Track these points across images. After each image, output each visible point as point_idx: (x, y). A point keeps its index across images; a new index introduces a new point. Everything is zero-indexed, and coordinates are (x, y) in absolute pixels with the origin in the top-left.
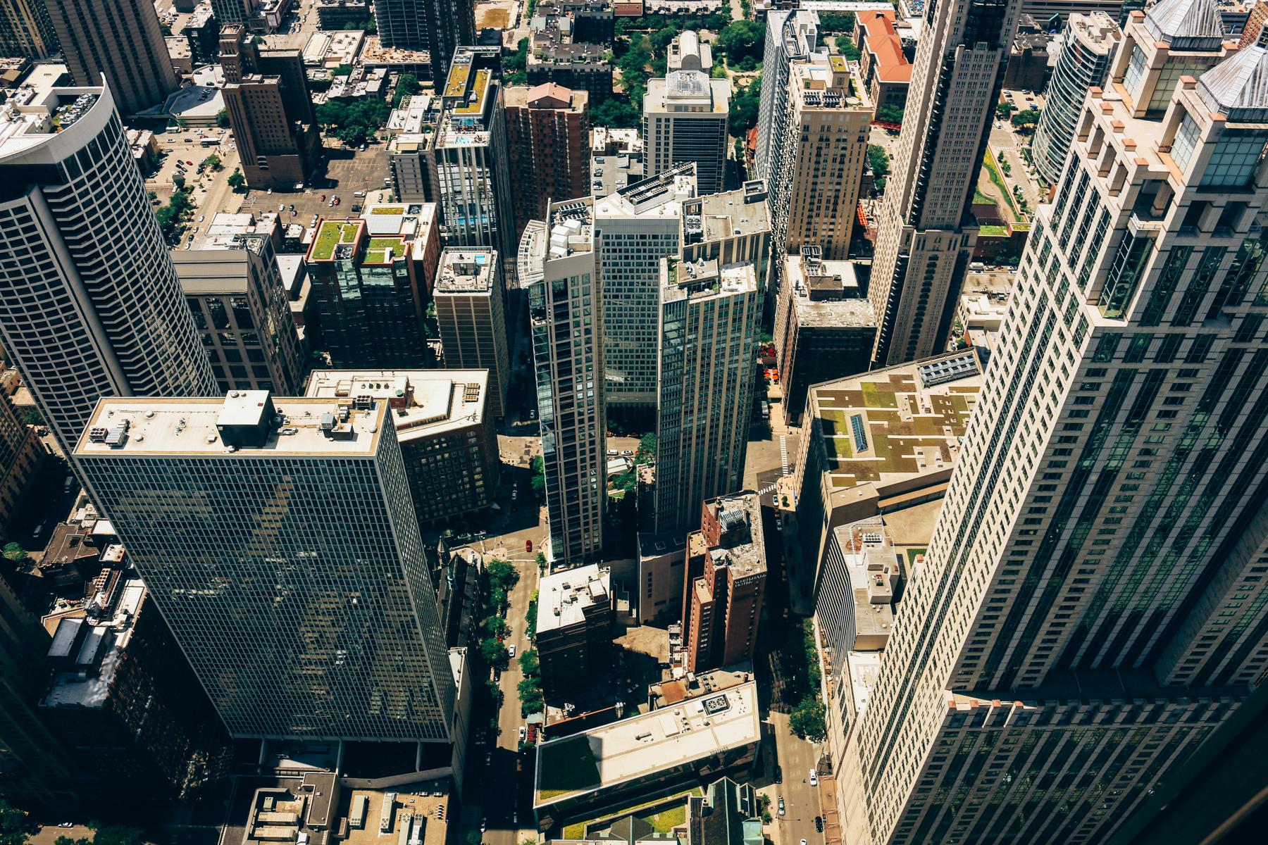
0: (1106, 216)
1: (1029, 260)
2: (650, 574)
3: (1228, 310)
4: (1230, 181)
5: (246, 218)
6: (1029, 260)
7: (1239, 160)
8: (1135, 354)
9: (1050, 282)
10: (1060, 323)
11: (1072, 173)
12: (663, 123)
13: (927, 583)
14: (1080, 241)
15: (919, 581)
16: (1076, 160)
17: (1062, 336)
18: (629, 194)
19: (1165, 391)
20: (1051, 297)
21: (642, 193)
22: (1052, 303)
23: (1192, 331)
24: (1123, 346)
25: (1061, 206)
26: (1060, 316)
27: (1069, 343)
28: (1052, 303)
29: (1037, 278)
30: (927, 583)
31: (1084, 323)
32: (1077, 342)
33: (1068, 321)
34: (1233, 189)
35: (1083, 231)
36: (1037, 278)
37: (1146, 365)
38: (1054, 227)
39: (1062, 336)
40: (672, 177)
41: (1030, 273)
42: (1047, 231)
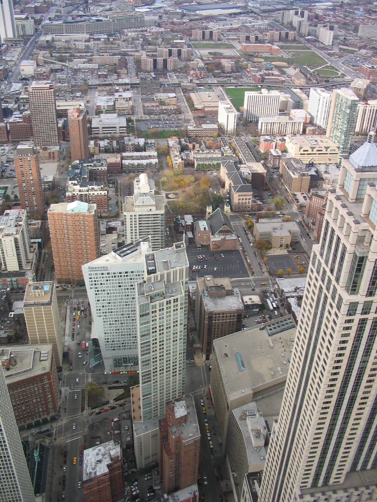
0: (344, 248)
1: (312, 271)
2: (141, 443)
6: (312, 271)
9: (323, 281)
10: (329, 300)
11: (327, 229)
12: (133, 217)
13: (281, 434)
15: (277, 433)
17: (331, 306)
18: (118, 252)
20: (324, 287)
21: (125, 251)
22: (325, 291)
24: (360, 308)
25: (323, 246)
26: (329, 296)
27: (335, 309)
28: (325, 291)
29: (317, 280)
30: (281, 434)
31: (340, 299)
32: (339, 308)
35: (335, 256)
36: (317, 280)
38: (321, 255)
39: (331, 306)
40: (139, 242)
41: (313, 277)
42: (319, 257)
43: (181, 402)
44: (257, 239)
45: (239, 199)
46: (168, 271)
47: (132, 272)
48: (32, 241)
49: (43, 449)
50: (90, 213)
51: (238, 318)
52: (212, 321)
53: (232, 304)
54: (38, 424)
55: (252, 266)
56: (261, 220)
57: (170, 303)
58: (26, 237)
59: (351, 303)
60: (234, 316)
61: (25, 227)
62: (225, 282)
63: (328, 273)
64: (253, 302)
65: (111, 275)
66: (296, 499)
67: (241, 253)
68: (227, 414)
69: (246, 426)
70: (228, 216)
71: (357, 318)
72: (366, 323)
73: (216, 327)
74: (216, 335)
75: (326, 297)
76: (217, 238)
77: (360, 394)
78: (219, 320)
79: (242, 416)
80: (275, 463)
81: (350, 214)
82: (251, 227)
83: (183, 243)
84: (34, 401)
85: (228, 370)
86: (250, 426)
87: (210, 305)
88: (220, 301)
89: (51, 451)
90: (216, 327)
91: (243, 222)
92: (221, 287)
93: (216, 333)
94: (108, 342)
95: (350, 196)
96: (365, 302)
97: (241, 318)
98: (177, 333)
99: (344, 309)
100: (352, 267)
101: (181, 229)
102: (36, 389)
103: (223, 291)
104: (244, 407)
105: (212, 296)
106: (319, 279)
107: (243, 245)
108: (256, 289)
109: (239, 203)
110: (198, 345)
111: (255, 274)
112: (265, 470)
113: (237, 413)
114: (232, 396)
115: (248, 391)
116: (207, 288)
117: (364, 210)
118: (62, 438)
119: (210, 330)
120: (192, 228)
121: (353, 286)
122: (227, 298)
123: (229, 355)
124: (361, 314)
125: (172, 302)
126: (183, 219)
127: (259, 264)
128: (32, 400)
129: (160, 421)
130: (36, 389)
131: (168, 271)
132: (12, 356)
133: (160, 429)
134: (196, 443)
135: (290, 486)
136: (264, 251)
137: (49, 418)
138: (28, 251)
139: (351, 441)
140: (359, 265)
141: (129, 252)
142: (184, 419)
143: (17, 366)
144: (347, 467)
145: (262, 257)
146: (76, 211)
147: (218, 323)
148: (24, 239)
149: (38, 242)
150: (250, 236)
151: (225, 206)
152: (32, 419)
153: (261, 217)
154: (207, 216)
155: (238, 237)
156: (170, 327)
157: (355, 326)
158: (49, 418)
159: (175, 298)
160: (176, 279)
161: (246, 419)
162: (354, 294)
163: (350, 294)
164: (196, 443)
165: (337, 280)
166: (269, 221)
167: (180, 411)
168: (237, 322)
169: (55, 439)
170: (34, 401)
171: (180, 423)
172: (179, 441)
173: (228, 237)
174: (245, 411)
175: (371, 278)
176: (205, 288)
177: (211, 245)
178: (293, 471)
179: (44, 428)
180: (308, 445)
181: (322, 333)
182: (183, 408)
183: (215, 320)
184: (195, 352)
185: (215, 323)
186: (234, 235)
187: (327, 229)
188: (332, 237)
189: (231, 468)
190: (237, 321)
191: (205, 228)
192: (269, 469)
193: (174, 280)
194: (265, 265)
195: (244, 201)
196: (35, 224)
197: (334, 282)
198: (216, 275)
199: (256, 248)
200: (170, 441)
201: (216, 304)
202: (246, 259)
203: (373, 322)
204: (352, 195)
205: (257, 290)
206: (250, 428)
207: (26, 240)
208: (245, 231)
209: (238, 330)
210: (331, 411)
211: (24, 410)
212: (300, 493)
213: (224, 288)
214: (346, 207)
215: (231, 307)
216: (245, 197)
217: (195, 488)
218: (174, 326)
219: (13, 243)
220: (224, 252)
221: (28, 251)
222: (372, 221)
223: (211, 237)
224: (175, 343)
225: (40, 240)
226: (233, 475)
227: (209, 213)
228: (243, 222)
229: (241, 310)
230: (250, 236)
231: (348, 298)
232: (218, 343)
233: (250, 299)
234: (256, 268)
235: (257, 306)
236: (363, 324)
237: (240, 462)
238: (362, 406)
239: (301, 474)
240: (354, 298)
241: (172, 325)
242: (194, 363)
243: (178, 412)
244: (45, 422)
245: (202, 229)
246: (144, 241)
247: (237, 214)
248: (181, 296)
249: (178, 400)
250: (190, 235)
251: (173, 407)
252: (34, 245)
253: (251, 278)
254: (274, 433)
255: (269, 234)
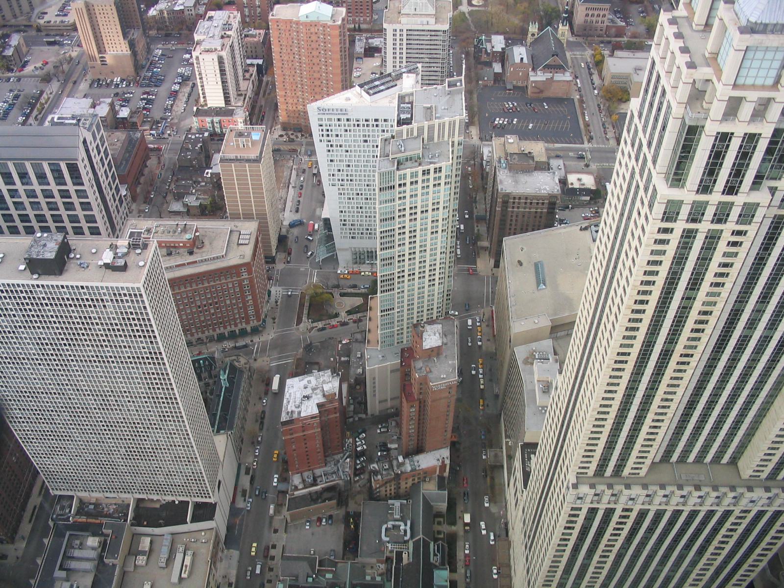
1: (626, 142)
3: (773, 183)
4: (759, 82)
5: (89, 101)
7: (766, 64)
8: (696, 216)
10: (641, 192)
11: (651, 73)
12: (398, 33)
14: (654, 128)
16: (653, 63)
18: (366, 87)
19: (722, 246)
20: (637, 171)
21: (377, 86)
22: (637, 176)
23: (739, 200)
25: (644, 101)
27: (646, 208)
28: (637, 176)
29: (630, 157)
30: (563, 392)
32: (651, 206)
33: (646, 189)
34: (763, 87)
36: (630, 157)
37: (704, 227)
40: (401, 74)
43: (436, 326)
44: (606, 83)
45: (587, 15)
46: (431, 123)
47: (385, 120)
48: (249, 61)
49: (234, 371)
50: (334, 21)
51: (549, 208)
52: (507, 208)
53: (543, 184)
54: (233, 336)
55: (591, 128)
56: (618, 53)
57: (429, 173)
58: (238, 56)
59: (669, 201)
60: (543, 204)
61: (236, 40)
62: (538, 149)
63: (645, 148)
64: (583, 185)
65: (352, 123)
66: (568, 488)
67: (577, 104)
68: (509, 352)
69: (532, 373)
70: (564, 42)
71: (680, 226)
72: (695, 237)
73: (514, 218)
74: (512, 230)
75: (638, 187)
76: (539, 77)
77: (679, 349)
78: (518, 208)
79: (528, 358)
80: (552, 434)
81: (685, 50)
82: (599, 64)
83: (461, 81)
84: (228, 302)
85: (517, 283)
86: (534, 375)
87: (507, 183)
88: (523, 178)
89: (245, 376)
90: (514, 218)
91: (589, 53)
92: (529, 156)
93: (513, 227)
94: (344, 225)
95: (696, 19)
96: (720, 203)
97: (554, 209)
98: (437, 221)
99: (659, 209)
100: (677, 142)
101: (484, 58)
102: (230, 286)
103: (531, 162)
104: (534, 346)
105: (511, 168)
106: (633, 156)
107: (583, 92)
108: (591, 164)
109: (586, 21)
110: (485, 244)
111: (594, 141)
112: (540, 442)
113: (520, 353)
114: (518, 327)
115: (545, 322)
116: (506, 154)
117: (710, 46)
118: (265, 359)
119: (503, 221)
120: (502, 57)
121: (675, 174)
122: (536, 173)
123: (525, 264)
124: (687, 221)
125: (432, 171)
126: (490, 41)
127: (603, 125)
128: (225, 300)
129: (403, 350)
130: (230, 286)
131: (431, 123)
132: (197, 234)
133: (402, 362)
134: (450, 388)
135: (564, 469)
136: (616, 104)
137: (249, 329)
138: (241, 78)
139: (661, 417)
140: (686, 140)
141: (382, 88)
142: (436, 352)
143: (204, 250)
144: (655, 452)
145: (610, 113)
146: (313, 18)
147: (518, 213)
148: (233, 58)
149: (258, 65)
150: (595, 77)
151: (560, 25)
152: (225, 327)
153: (617, 47)
154: (530, 39)
155: (577, 77)
156: (427, 211)
157: (675, 239)
158: (249, 329)
159: (437, 166)
160: (443, 136)
161: (532, 364)
162: (678, 186)
163: (672, 186)
164: (450, 388)
165: (654, 162)
166: (631, 55)
167: (432, 339)
168: (545, 214)
169: (255, 360)
170: (228, 302)
171: (430, 357)
172: (424, 381)
173: (559, 77)
174: (534, 351)
175: (734, 164)
176: (503, 155)
177: (529, 88)
178: (571, 450)
179: (241, 343)
180: (592, 414)
181: (626, 246)
182: (437, 335)
183: (513, 207)
184: (478, 253)
185: (512, 212)
186: (568, 74)
187: (651, 73)
188: (656, 88)
189: (506, 431)
190: (548, 213)
191: (522, 59)
192: (545, 441)
193: (439, 137)
194: (614, 128)
195: (594, 19)
196: (254, 36)
197: (649, 163)
198: (524, 135)
199: (602, 97)
200: (413, 381)
201: (516, 182)
202: (583, 114)
203: (706, 237)
204: (699, 18)
205: (594, 166)
206: (536, 377)
207: (238, 59)
208: (589, 69)
209: (549, 225)
210: (629, 367)
211: (213, 314)
212: (575, 481)
213: (533, 158)
214: (682, 37)
215: (540, 190)
216: (596, 13)
217: (445, 453)
218: (433, 210)
219: (217, 63)
220: (549, 100)
221: (241, 78)
222: (721, 65)
223: (531, 73)
224: (434, 235)
225: (260, 62)
226: (507, 443)
227: (533, 35)
228: (589, 53)
229: (555, 197)
230: (595, 77)
231: (666, 192)
232: (511, 244)
233: (579, 180)
234: (596, 129)
235: (588, 191)
236: (689, 237)
237: (516, 424)
238: (682, 367)
239: (578, 454)
240: (676, 194)
241: (430, 208)
242: (476, 271)
243: (428, 341)
244: (243, 333)
245: (517, 60)
246: (409, 72)
247: (580, 39)
248: (448, 164)
249: (431, 322)
250: (497, 68)
251: (423, 332)
252: (251, 69)
253: (586, 145)
254: (556, 388)
255: (627, 77)
